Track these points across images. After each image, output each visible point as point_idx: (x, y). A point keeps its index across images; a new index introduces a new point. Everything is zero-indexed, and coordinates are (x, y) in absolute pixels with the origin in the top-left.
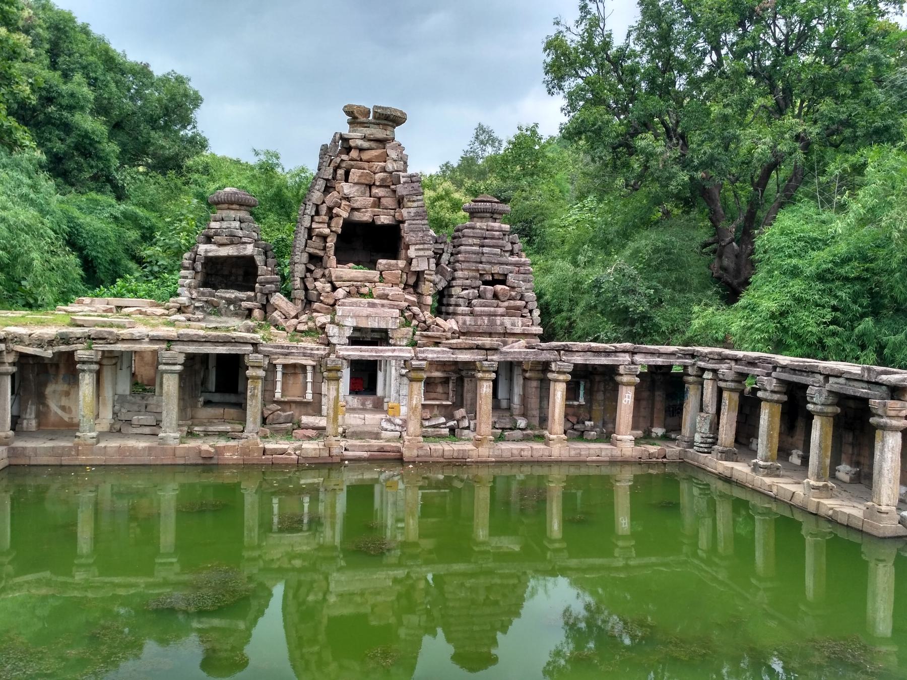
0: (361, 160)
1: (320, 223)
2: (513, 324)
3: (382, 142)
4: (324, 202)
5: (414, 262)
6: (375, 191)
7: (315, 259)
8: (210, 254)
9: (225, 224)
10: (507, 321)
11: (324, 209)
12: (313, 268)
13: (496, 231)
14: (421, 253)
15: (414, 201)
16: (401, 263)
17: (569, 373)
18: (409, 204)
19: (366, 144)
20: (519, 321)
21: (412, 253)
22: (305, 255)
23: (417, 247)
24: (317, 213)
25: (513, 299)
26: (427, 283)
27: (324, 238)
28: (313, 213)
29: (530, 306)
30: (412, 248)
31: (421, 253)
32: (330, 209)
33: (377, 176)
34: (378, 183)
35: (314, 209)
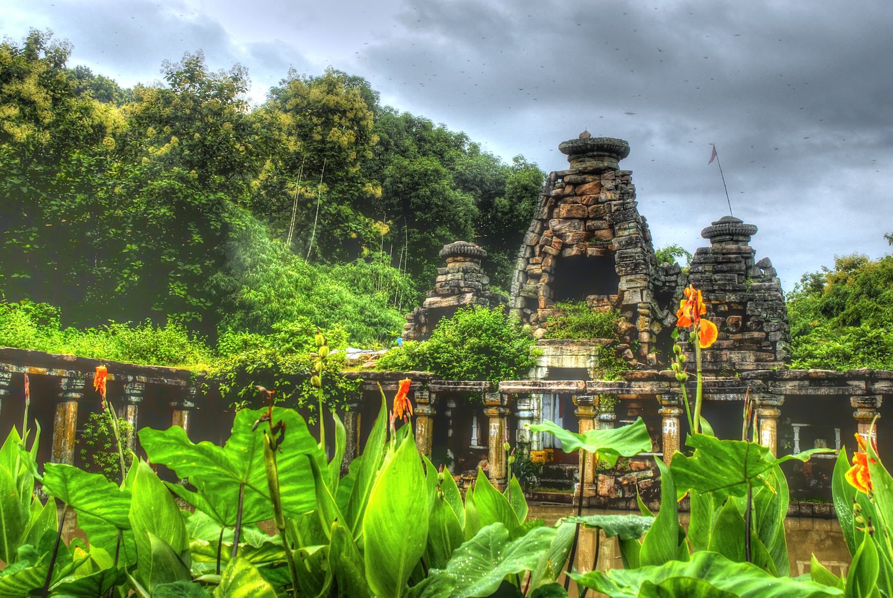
0: (576, 195)
1: (534, 264)
2: (743, 359)
3: (598, 172)
4: (538, 243)
5: (626, 295)
6: (589, 223)
7: (531, 303)
8: (434, 306)
9: (449, 277)
10: (735, 356)
11: (537, 249)
12: (529, 312)
13: (734, 253)
14: (633, 285)
15: (625, 229)
16: (614, 297)
17: (778, 407)
18: (620, 233)
19: (579, 178)
20: (751, 357)
21: (623, 285)
22: (520, 300)
23: (629, 277)
24: (533, 254)
25: (749, 330)
26: (641, 317)
27: (537, 277)
28: (528, 255)
29: (772, 337)
30: (623, 280)
31: (633, 285)
32: (542, 247)
33: (590, 208)
34: (591, 216)
35: (529, 251)
